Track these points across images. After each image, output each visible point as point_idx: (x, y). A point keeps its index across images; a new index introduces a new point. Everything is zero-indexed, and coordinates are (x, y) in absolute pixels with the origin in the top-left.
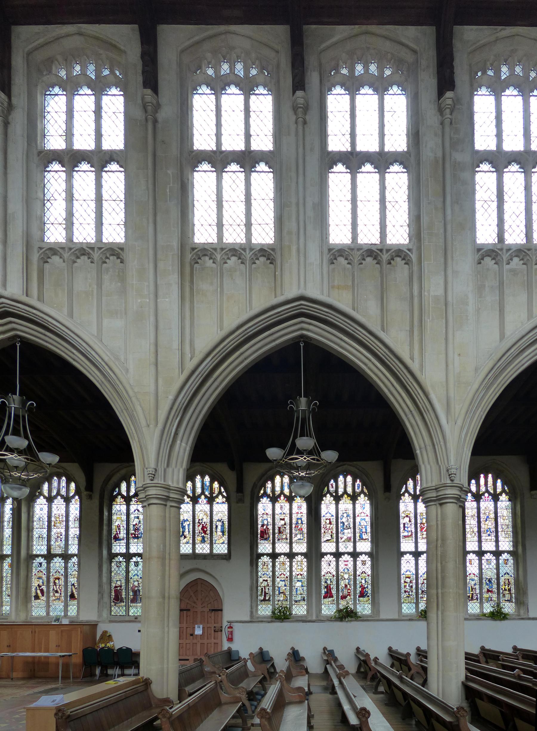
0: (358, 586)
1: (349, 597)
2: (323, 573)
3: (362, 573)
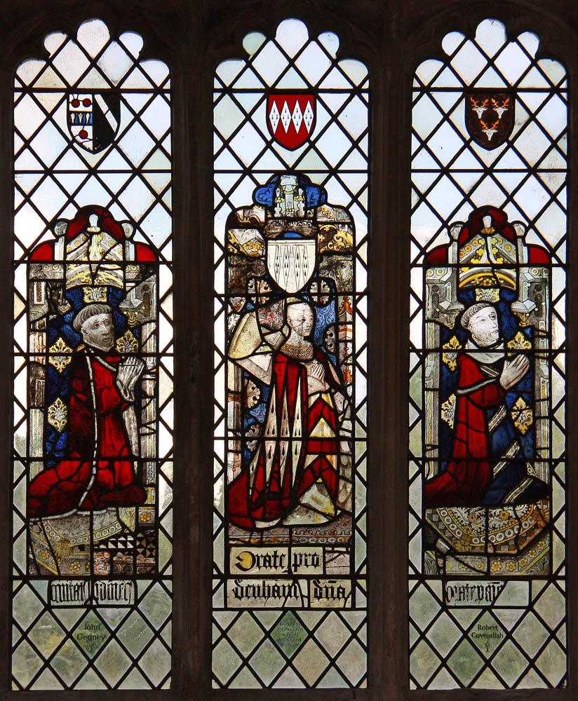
0: (423, 378)
1: (313, 495)
2: (27, 228)
3: (472, 229)
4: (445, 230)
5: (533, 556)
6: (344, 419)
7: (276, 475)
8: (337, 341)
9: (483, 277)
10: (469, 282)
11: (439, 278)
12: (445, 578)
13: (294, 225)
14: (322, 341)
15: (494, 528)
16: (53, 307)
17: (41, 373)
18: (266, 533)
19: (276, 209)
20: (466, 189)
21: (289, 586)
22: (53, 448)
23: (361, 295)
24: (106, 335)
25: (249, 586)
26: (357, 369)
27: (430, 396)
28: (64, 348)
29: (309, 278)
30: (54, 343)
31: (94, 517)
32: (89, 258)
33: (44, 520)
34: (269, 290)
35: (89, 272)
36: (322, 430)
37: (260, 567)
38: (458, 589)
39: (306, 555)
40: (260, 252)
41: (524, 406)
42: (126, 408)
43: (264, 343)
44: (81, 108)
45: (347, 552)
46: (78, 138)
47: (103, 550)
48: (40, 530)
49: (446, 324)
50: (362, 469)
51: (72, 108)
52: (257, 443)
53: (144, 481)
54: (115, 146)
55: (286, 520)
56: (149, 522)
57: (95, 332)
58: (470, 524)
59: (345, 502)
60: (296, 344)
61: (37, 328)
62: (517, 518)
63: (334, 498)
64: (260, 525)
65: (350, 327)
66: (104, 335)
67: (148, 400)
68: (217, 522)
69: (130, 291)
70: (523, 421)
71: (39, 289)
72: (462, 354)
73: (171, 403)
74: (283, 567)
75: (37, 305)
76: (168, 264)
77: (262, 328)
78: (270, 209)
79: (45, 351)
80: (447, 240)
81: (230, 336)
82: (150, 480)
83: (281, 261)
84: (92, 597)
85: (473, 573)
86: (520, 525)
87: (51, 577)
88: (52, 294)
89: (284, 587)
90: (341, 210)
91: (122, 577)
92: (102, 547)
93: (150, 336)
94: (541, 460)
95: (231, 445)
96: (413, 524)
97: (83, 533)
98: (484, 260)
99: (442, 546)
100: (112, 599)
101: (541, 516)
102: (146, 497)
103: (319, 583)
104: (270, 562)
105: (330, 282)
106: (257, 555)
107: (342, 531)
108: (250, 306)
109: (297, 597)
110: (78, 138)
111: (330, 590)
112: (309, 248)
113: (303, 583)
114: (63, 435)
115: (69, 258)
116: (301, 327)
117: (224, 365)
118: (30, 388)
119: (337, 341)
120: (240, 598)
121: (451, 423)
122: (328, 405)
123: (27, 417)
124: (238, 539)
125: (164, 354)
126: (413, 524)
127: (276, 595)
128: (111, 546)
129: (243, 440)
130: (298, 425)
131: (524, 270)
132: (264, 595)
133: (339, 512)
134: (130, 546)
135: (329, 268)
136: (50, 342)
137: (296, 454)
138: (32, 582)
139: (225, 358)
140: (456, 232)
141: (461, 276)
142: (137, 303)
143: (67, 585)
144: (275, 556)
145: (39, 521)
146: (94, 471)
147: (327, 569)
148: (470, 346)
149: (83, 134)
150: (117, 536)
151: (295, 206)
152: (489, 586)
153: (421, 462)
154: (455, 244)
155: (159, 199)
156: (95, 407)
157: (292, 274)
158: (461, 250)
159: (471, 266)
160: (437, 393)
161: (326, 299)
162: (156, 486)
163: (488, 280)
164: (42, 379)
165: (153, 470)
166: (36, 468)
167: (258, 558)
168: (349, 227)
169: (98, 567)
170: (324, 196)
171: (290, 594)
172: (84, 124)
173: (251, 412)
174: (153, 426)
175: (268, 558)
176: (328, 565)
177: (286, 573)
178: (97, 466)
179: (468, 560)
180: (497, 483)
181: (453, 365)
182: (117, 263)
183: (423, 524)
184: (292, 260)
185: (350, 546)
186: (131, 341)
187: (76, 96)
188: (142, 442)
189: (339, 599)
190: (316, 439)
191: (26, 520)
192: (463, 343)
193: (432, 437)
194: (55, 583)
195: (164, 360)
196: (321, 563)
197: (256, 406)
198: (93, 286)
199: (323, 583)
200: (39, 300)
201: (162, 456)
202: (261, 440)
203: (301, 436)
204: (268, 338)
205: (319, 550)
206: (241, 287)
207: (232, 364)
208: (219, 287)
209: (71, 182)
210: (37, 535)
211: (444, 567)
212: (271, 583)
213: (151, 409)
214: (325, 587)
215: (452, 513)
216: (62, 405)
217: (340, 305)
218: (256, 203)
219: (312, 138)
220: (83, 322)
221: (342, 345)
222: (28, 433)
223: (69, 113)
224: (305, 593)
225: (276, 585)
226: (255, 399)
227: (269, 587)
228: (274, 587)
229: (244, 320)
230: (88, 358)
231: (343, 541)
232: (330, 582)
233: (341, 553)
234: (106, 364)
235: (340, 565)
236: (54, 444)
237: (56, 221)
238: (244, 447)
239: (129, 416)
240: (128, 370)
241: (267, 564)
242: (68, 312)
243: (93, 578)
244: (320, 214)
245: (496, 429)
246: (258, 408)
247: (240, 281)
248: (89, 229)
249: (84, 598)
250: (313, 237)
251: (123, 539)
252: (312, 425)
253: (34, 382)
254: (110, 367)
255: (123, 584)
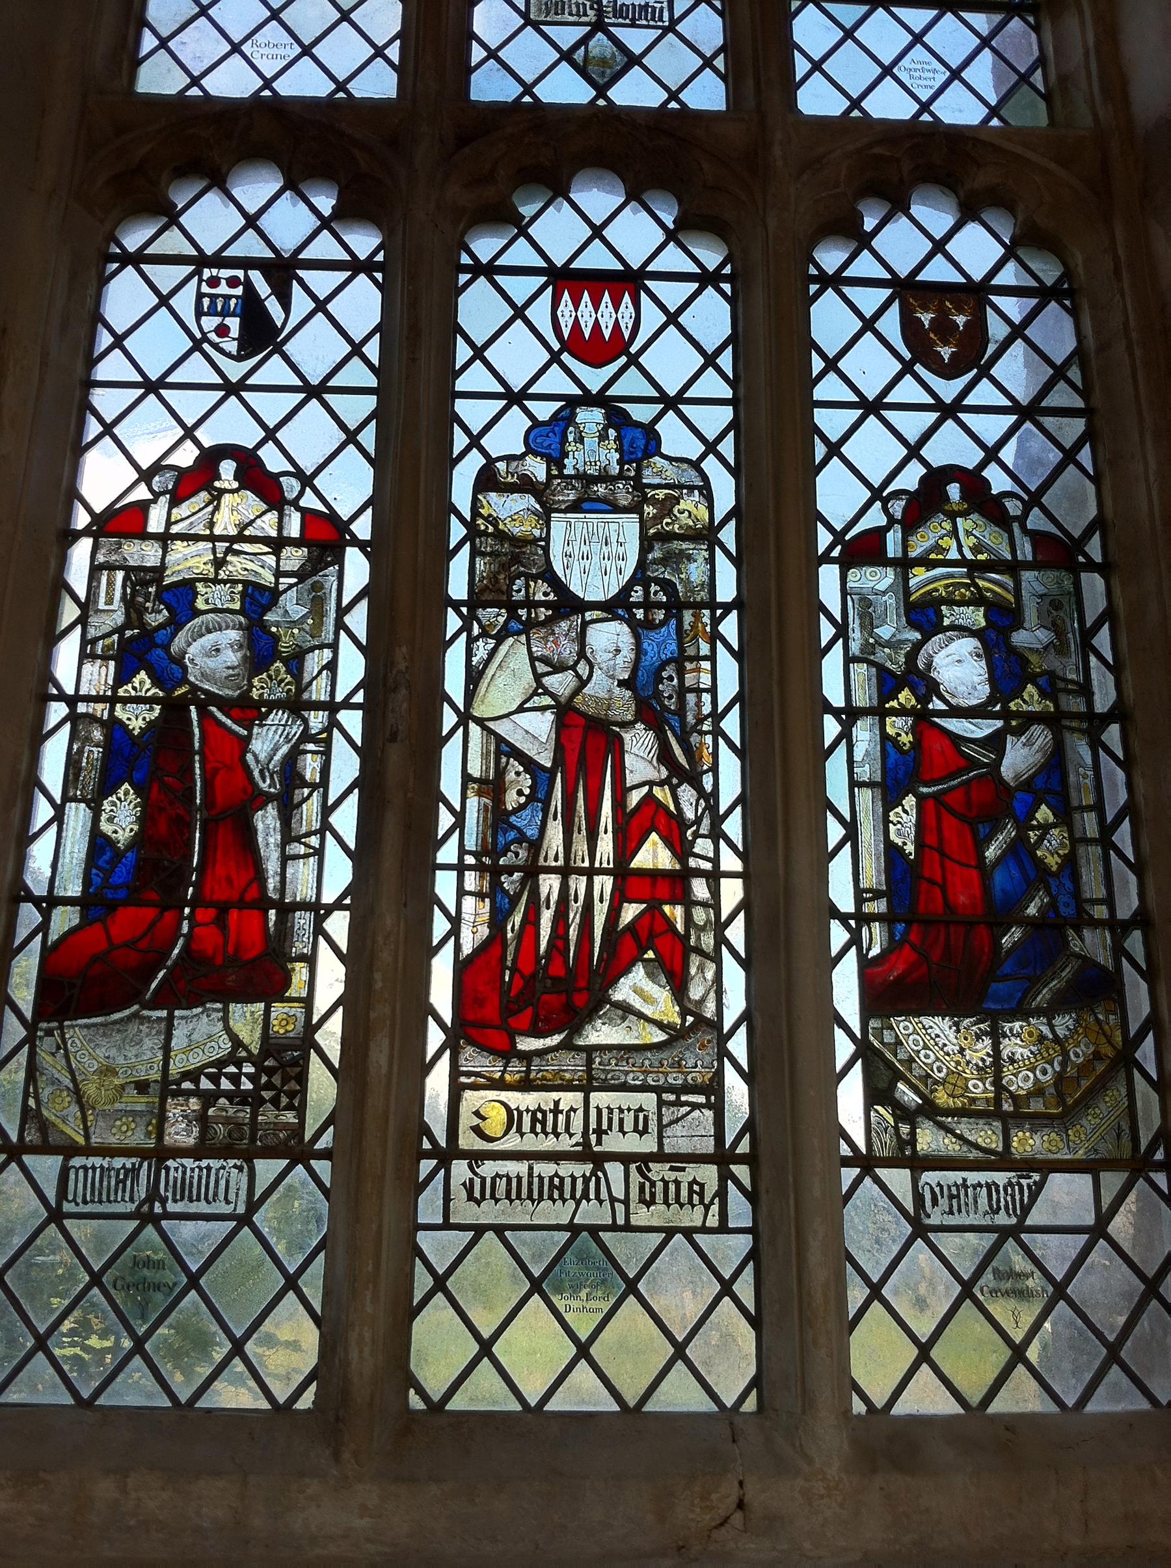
1: (637, 986)
2: (103, 479)
4: (878, 504)
5: (1098, 1121)
6: (697, 835)
7: (560, 943)
8: (682, 691)
9: (952, 584)
10: (929, 593)
11: (871, 585)
12: (918, 1164)
13: (601, 489)
14: (651, 689)
15: (1012, 1061)
16: (134, 615)
17: (97, 735)
18: (536, 1061)
19: (566, 461)
20: (912, 439)
21: (584, 1176)
22: (105, 879)
23: (727, 608)
24: (233, 668)
25: (497, 1175)
26: (721, 741)
27: (865, 797)
28: (148, 690)
29: (626, 580)
30: (129, 680)
31: (176, 1023)
32: (211, 531)
33: (68, 1026)
34: (551, 597)
35: (212, 557)
36: (655, 856)
37: (522, 1135)
38: (945, 1189)
39: (621, 1111)
40: (537, 533)
41: (1051, 819)
42: (263, 806)
43: (540, 691)
44: (223, 289)
45: (707, 1105)
46: (213, 336)
47: (188, 1094)
48: (58, 1048)
49: (888, 664)
50: (736, 933)
51: (205, 289)
52: (523, 878)
53: (288, 950)
54: (279, 350)
55: (580, 1035)
56: (291, 1035)
57: (211, 663)
58: (962, 1051)
59: (703, 1000)
60: (603, 694)
61: (99, 652)
62: (1056, 1039)
63: (679, 988)
64: (527, 1044)
65: (706, 665)
66: (228, 668)
67: (306, 791)
68: (435, 1037)
69: (285, 591)
70: (1051, 850)
71: (110, 584)
72: (922, 718)
73: (354, 798)
74: (571, 1135)
75: (104, 611)
76: (362, 545)
77: (537, 663)
78: (556, 461)
79: (109, 693)
80: (883, 521)
81: (474, 677)
82: (301, 947)
83: (576, 548)
84: (153, 1195)
85: (974, 1154)
86: (1065, 1053)
87: (69, 1150)
88: (134, 593)
89: (574, 1179)
90: (685, 466)
91: (224, 1152)
92: (187, 1085)
93: (320, 673)
94: (1096, 924)
95: (471, 881)
96: (844, 1048)
97: (149, 1054)
98: (953, 555)
99: (906, 1094)
100: (198, 1200)
101: (1104, 1034)
102: (287, 982)
103: (649, 1170)
104: (544, 1123)
105: (667, 586)
106: (517, 1109)
107: (696, 1062)
108: (515, 625)
109: (601, 1202)
110: (213, 336)
111: (672, 1187)
112: (630, 526)
113: (615, 1170)
114: (129, 854)
115: (175, 529)
116: (612, 662)
117: (461, 729)
118: (73, 763)
119: (682, 691)
120: (478, 1203)
121: (910, 848)
122: (666, 808)
123: (59, 817)
124: (477, 1074)
125: (347, 704)
126: (844, 1048)
127: (556, 1195)
128: (205, 1084)
129: (495, 872)
130: (606, 846)
131: (1027, 576)
132: (530, 1197)
133: (690, 1019)
134: (246, 1085)
135: (664, 561)
136: (122, 678)
137: (601, 901)
138: (26, 1159)
139: (465, 718)
140: (897, 508)
141: (912, 582)
142: (297, 611)
143: (102, 1167)
144: (556, 1111)
145: (57, 1029)
146: (185, 928)
147: (666, 1141)
148: (937, 704)
149: (222, 331)
150: (220, 1063)
151: (603, 458)
152: (1010, 1184)
153: (852, 923)
154: (898, 527)
155: (351, 437)
156: (198, 801)
157: (595, 572)
158: (910, 538)
159: (931, 565)
160: (878, 791)
161: (660, 615)
162: (311, 960)
163: (963, 590)
164: (97, 746)
165: (306, 927)
166: (64, 920)
167: (520, 1114)
168: (701, 493)
169: (172, 1130)
170: (653, 443)
171: (585, 1195)
172: (225, 313)
173: (513, 819)
174: (314, 841)
175: (539, 1115)
176: (668, 1132)
177: (580, 1148)
178: (190, 918)
179: (963, 1127)
180: (1006, 968)
181: (906, 739)
182: (265, 540)
183: (864, 1051)
184: (596, 547)
185: (714, 1089)
186: (282, 681)
187: (215, 272)
188: (290, 871)
189: (693, 1206)
190: (642, 872)
191: (31, 1027)
192: (924, 699)
193: (872, 876)
194: (77, 1162)
195: (343, 716)
196: (653, 1126)
197: (522, 807)
198: (216, 581)
199: (658, 1171)
200: (109, 601)
201: (328, 898)
202: (532, 872)
203: (611, 866)
204: (546, 681)
205: (648, 1100)
206: (500, 591)
207: (478, 728)
208: (458, 588)
209: (190, 405)
210: (49, 1058)
211: (913, 1141)
212: (545, 1169)
213: (311, 810)
214: (663, 1180)
215: (924, 1027)
216: (132, 796)
217: (687, 627)
218: (530, 450)
219: (633, 349)
220: (189, 645)
221: (691, 698)
222: (54, 855)
223: (200, 296)
224: (619, 1192)
225: (556, 1175)
226: (520, 793)
227: (541, 1178)
228: (551, 1179)
229: (504, 649)
230: (192, 708)
231: (699, 1080)
232: (672, 1169)
233: (695, 1106)
234: (229, 722)
235: (692, 1131)
236: (108, 873)
237: (158, 467)
238: (496, 885)
239: (267, 821)
240: (271, 733)
241: (539, 1127)
242: (161, 626)
243: (161, 1154)
244: (646, 472)
245: (999, 860)
246: (527, 812)
247: (497, 581)
248: (217, 484)
249: (136, 1198)
250: (635, 508)
251: (232, 1069)
252: (633, 845)
253: (80, 751)
254: (235, 727)
255: (223, 1168)
